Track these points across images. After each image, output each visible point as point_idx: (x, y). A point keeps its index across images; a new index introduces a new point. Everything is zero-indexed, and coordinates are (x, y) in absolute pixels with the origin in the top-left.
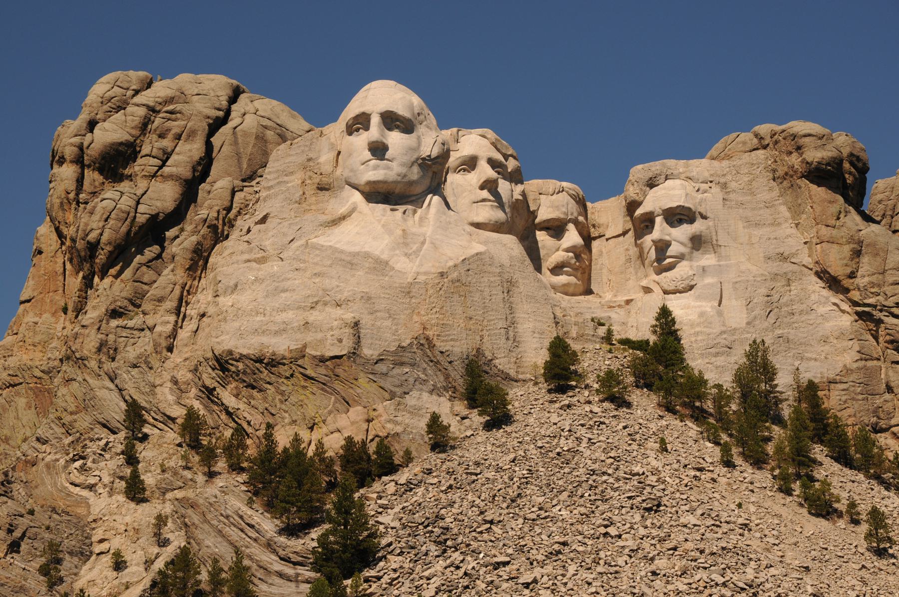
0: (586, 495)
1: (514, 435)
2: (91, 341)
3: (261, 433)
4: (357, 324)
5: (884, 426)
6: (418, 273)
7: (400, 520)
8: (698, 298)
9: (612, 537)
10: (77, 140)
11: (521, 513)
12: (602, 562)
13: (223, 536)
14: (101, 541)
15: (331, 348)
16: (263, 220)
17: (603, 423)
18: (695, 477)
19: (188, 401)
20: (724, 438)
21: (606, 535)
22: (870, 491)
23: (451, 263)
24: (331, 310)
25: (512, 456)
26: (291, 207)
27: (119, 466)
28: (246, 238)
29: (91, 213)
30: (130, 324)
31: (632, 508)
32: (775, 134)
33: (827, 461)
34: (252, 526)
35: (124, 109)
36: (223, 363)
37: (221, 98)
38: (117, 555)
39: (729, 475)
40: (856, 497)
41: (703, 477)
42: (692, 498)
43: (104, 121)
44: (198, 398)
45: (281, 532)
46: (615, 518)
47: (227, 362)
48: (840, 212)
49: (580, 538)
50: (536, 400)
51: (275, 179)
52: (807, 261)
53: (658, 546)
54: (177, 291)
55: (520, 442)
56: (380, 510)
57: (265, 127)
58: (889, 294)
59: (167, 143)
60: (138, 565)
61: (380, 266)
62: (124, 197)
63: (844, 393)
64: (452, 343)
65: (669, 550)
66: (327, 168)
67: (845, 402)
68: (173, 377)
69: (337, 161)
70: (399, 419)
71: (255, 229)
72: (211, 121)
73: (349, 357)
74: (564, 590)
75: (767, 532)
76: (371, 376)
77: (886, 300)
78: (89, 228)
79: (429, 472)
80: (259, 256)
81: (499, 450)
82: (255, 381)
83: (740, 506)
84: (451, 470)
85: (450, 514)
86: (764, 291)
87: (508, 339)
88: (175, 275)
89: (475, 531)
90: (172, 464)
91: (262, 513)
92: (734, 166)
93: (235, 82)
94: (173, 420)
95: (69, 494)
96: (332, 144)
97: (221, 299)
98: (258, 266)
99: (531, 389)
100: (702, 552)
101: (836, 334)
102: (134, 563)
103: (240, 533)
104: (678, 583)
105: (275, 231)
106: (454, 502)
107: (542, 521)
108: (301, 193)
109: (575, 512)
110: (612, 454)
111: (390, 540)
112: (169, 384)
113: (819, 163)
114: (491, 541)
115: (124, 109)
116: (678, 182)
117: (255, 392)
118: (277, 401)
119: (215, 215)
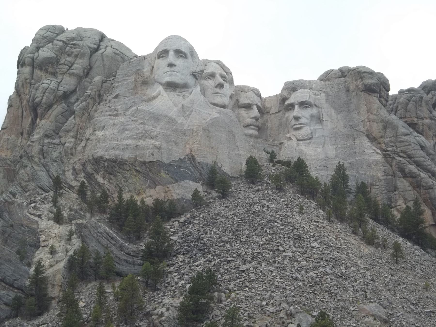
0: (268, 231)
2: (36, 149)
3: (115, 195)
5: (393, 206)
6: (189, 125)
7: (182, 238)
9: (281, 251)
10: (31, 55)
12: (277, 262)
13: (99, 242)
14: (44, 241)
16: (117, 97)
17: (272, 198)
19: (80, 179)
21: (278, 250)
23: (204, 122)
24: (148, 140)
25: (233, 212)
27: (51, 207)
28: (108, 105)
29: (37, 89)
30: (54, 142)
31: (289, 238)
33: (370, 220)
35: (52, 42)
36: (97, 161)
37: (96, 39)
38: (52, 247)
39: (330, 225)
40: (385, 237)
42: (316, 235)
43: (43, 47)
44: (84, 177)
49: (266, 251)
50: (242, 187)
52: (362, 129)
53: (302, 256)
54: (76, 128)
57: (116, 54)
60: (61, 253)
61: (171, 121)
62: (52, 83)
65: (307, 258)
66: (147, 74)
67: (377, 194)
68: (73, 167)
69: (152, 71)
70: (179, 192)
74: (260, 274)
75: (349, 251)
76: (166, 172)
77: (397, 148)
78: (36, 96)
79: (194, 217)
80: (115, 113)
81: (226, 209)
83: (336, 239)
86: (343, 142)
88: (75, 120)
90: (75, 207)
92: (331, 84)
94: (73, 187)
95: (29, 219)
96: (150, 63)
97: (97, 132)
100: (321, 259)
102: (59, 251)
103: (107, 241)
104: (311, 273)
106: (207, 232)
109: (263, 239)
111: (178, 248)
112: (71, 171)
113: (370, 85)
114: (225, 250)
115: (52, 42)
116: (306, 90)
117: (112, 177)
119: (94, 93)
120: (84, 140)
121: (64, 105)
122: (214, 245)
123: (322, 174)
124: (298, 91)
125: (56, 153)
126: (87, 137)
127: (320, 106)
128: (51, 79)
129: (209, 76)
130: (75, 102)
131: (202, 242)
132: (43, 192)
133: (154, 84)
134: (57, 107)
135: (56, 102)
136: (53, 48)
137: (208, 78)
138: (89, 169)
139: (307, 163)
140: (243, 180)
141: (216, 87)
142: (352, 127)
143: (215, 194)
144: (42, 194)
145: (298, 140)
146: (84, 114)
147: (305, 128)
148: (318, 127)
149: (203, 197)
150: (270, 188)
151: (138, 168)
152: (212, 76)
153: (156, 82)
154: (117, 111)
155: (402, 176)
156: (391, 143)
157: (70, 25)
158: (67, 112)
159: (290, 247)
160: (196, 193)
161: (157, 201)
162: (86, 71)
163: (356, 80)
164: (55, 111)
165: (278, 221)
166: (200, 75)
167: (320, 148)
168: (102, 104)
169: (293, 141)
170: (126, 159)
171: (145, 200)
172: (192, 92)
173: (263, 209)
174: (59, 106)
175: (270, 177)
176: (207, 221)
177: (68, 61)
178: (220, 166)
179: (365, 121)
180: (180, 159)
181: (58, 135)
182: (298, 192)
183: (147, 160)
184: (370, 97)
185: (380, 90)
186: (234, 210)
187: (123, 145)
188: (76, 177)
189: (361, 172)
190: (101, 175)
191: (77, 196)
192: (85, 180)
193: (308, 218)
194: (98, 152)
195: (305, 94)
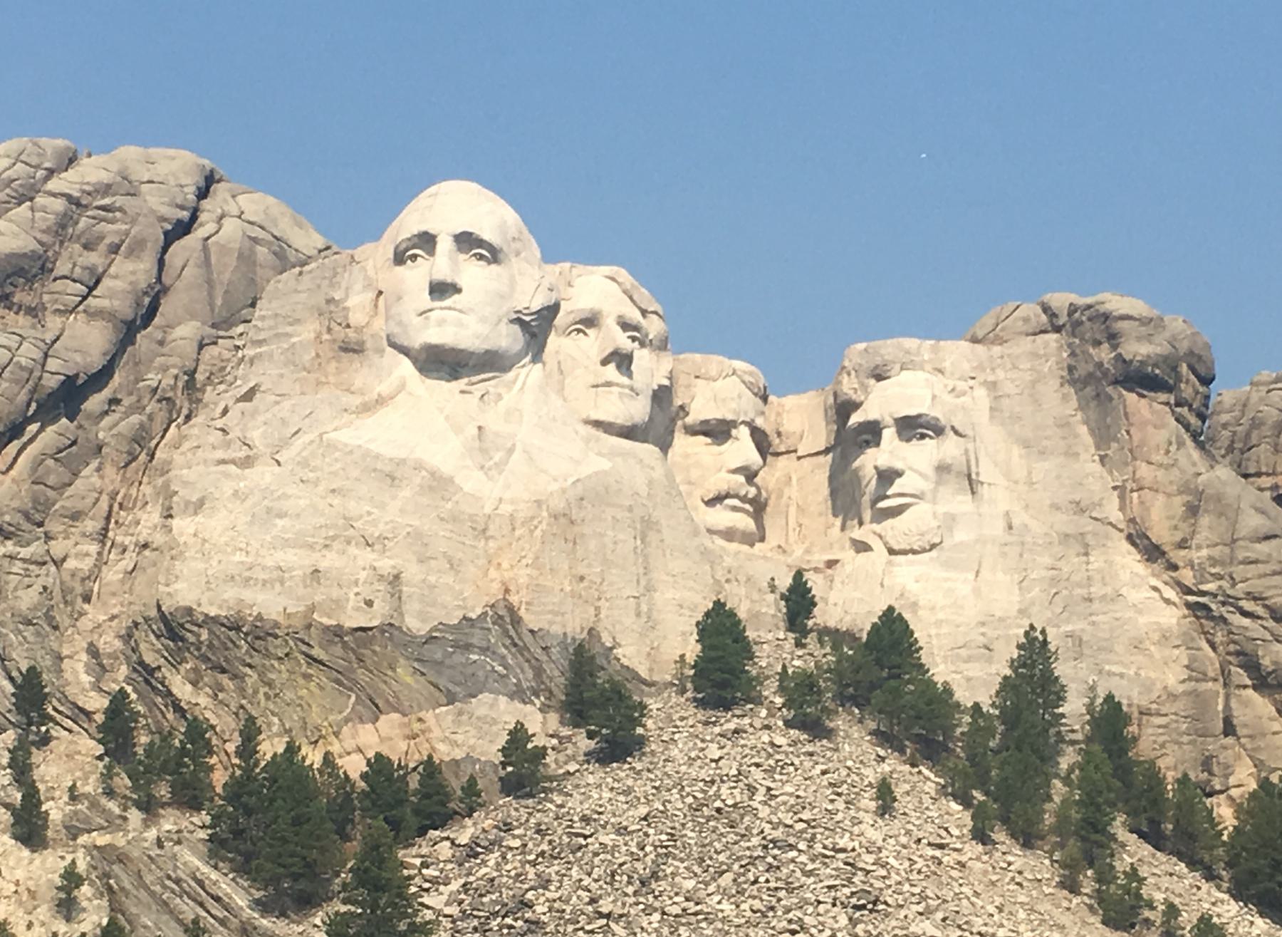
0: (762, 879)
1: (645, 774)
3: (231, 747)
4: (397, 577)
5: (1218, 787)
7: (461, 903)
8: (947, 565)
11: (657, 904)
13: (171, 912)
15: (355, 614)
16: (249, 396)
18: (933, 857)
20: (978, 795)
22: (1195, 890)
23: (555, 487)
24: (356, 552)
25: (643, 810)
26: (296, 376)
28: (219, 424)
30: (25, 552)
31: (834, 905)
32: (1076, 311)
34: (217, 899)
35: (31, 199)
39: (985, 858)
40: (1177, 901)
41: (945, 860)
44: (129, 680)
45: (263, 907)
46: (807, 919)
47: (182, 626)
48: (1170, 443)
51: (271, 328)
56: (427, 885)
57: (255, 240)
58: (1238, 579)
59: (95, 258)
61: (439, 484)
62: (25, 344)
63: (1161, 731)
64: (550, 616)
67: (1163, 746)
68: (91, 644)
69: (376, 306)
71: (236, 410)
72: (169, 227)
73: (383, 632)
76: (416, 665)
79: (507, 827)
81: (622, 798)
82: (227, 660)
84: (543, 827)
85: (542, 900)
86: (1047, 560)
87: (638, 615)
88: (102, 477)
89: (582, 929)
90: (89, 789)
91: (233, 880)
92: (1009, 355)
93: (207, 162)
94: (89, 715)
97: (176, 523)
98: (239, 471)
99: (674, 700)
101: (1156, 636)
105: (269, 415)
106: (549, 881)
107: (693, 919)
108: (313, 354)
110: (806, 815)
112: (84, 657)
115: (31, 199)
116: (920, 375)
117: (225, 680)
118: (261, 696)
119: (172, 382)
120: (132, 547)
123: (967, 672)
127: (970, 433)
129: (576, 323)
131: (527, 915)
136: (33, 219)
140: (689, 694)
141: (605, 362)
142: (1079, 508)
145: (892, 552)
148: (960, 503)
151: (317, 652)
152: (590, 321)
155: (1249, 682)
156: (1213, 566)
160: (518, 736)
161: (379, 766)
162: (147, 300)
168: (198, 420)
170: (274, 617)
171: (339, 762)
173: (751, 799)
176: (550, 842)
177: (84, 268)
178: (609, 645)
180: (465, 618)
183: (350, 623)
184: (1143, 401)
185: (1179, 378)
187: (264, 568)
188: (98, 681)
189: (1107, 667)
190: (187, 671)
191: (100, 750)
192: (129, 689)
193: (908, 833)
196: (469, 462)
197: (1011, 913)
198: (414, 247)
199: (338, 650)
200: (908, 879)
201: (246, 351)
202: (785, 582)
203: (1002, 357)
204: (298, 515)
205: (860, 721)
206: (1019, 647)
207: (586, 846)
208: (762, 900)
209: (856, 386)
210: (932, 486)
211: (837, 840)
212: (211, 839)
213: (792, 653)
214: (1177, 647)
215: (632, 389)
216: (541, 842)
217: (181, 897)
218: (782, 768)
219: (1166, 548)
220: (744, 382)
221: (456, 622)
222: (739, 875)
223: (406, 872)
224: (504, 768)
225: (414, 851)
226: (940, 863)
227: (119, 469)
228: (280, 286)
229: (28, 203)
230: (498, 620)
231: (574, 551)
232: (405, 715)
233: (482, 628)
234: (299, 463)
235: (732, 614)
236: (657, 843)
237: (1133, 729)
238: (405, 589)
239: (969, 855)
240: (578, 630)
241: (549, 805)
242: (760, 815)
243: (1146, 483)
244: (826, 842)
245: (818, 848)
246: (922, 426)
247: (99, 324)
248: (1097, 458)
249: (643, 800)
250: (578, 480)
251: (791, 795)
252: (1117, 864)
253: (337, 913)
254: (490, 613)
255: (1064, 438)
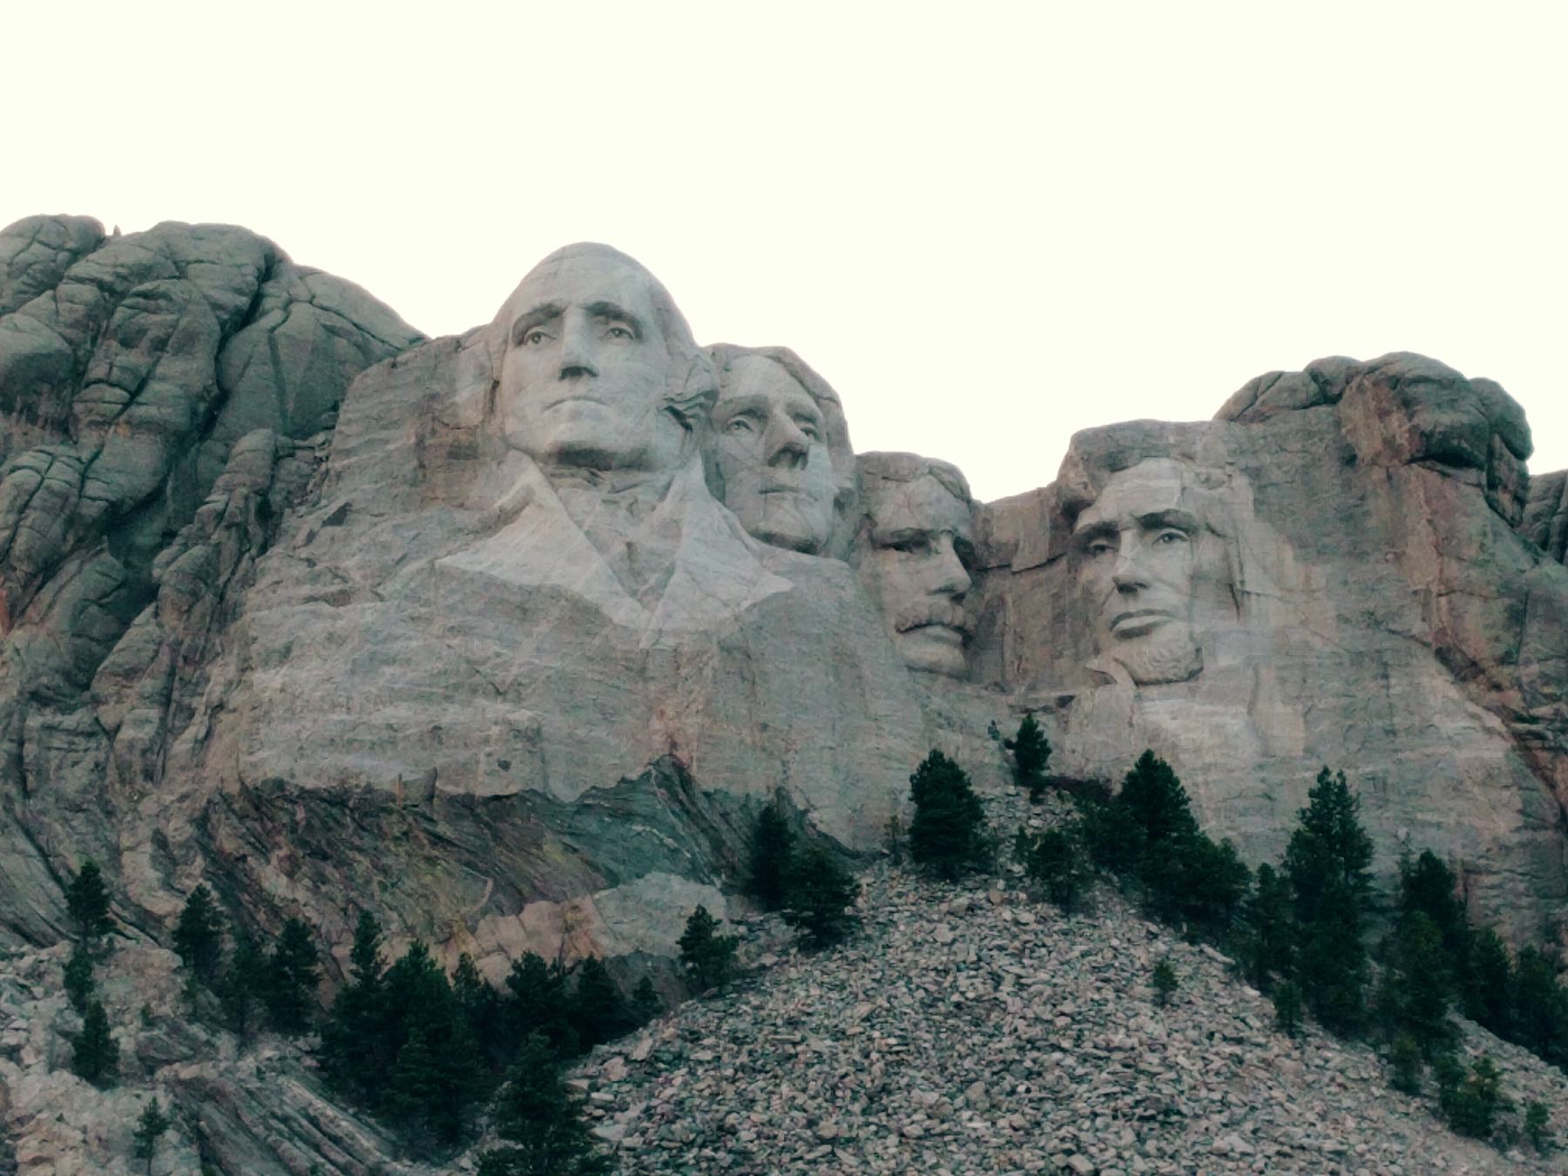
0: (1021, 1089)
1: (861, 965)
3: (343, 951)
6: (660, 631)
7: (643, 1133)
11: (893, 1124)
13: (279, 1159)
15: (487, 780)
16: (339, 518)
19: (187, 882)
22: (1557, 1088)
23: (726, 614)
25: (864, 1009)
26: (395, 491)
27: (61, 1011)
28: (304, 553)
31: (1115, 1118)
33: (1470, 1027)
35: (53, 287)
36: (262, 803)
37: (244, 270)
39: (1296, 1054)
40: (1540, 1100)
42: (1232, 1098)
43: (14, 311)
46: (1083, 1136)
50: (900, 895)
51: (359, 435)
52: (1418, 627)
54: (165, 657)
55: (878, 981)
56: (600, 1112)
57: (332, 331)
59: (135, 358)
61: (583, 616)
62: (57, 464)
63: (1494, 892)
66: (471, 416)
67: (1496, 911)
68: (157, 832)
69: (492, 401)
72: (226, 317)
76: (567, 840)
79: (694, 1037)
81: (835, 995)
82: (329, 844)
84: (741, 1035)
86: (1336, 685)
88: (160, 625)
89: (801, 1158)
90: (166, 1010)
94: (159, 920)
97: (258, 677)
99: (886, 873)
101: (1480, 775)
103: (313, 1154)
105: (365, 540)
106: (753, 1101)
108: (415, 463)
110: (1068, 1007)
112: (148, 848)
113: (1445, 436)
115: (53, 287)
116: (1165, 464)
117: (328, 869)
118: (375, 887)
119: (241, 504)
120: (202, 709)
121: (107, 557)
122: (786, 1157)
124: (1132, 470)
125: (78, 771)
126: (215, 700)
127: (1230, 532)
128: (49, 449)
130: (160, 547)
131: (730, 1145)
132: (27, 947)
133: (505, 454)
134: (80, 571)
135: (73, 550)
136: (57, 312)
137: (738, 423)
138: (228, 840)
139: (1186, 778)
141: (773, 462)
142: (1373, 621)
143: (781, 931)
144: (22, 956)
145: (1139, 683)
146: (195, 596)
147: (1169, 627)
148: (1225, 623)
149: (734, 942)
150: (1023, 896)
151: (443, 829)
152: (756, 412)
153: (510, 447)
154: (344, 580)
156: (1546, 684)
157: (127, 214)
158: (123, 592)
159: (1119, 1156)
160: (700, 924)
162: (202, 407)
163: (1383, 414)
164: (70, 588)
165: (1066, 1044)
166: (702, 414)
167: (1235, 716)
168: (276, 550)
169: (1117, 689)
170: (387, 787)
171: (479, 965)
172: (668, 487)
173: (996, 989)
174: (87, 567)
175: (1019, 846)
176: (750, 1053)
177: (124, 369)
178: (801, 807)
179: (1428, 591)
180: (623, 780)
181: (87, 695)
182: (1147, 912)
184: (1449, 482)
185: (1491, 453)
186: (868, 998)
187: (371, 727)
188: (169, 875)
190: (280, 860)
191: (178, 961)
192: (208, 885)
194: (263, 760)
195: (1163, 483)
196: (619, 588)
197: (1336, 1121)
198: (539, 324)
199: (468, 825)
200: (1206, 1084)
201: (330, 465)
202: (1011, 728)
203: (1264, 437)
204: (408, 661)
205: (1121, 891)
206: (1312, 794)
207: (796, 1055)
208: (1023, 1114)
209: (1085, 479)
210: (1186, 599)
211: (1111, 1036)
212: (323, 1067)
213: (1028, 810)
214: (1507, 787)
215: (809, 494)
216: (739, 1052)
217: (290, 1140)
218: (1033, 951)
219: (1485, 664)
220: (942, 483)
221: (613, 784)
222: (993, 1084)
223: (571, 1098)
224: (683, 964)
225: (579, 1071)
226: (1241, 1061)
227: (181, 613)
228: (369, 381)
229: (49, 293)
230: (665, 781)
231: (754, 694)
232: (557, 902)
233: (647, 793)
234: (407, 597)
235: (952, 765)
236: (885, 1049)
237: (1458, 891)
238: (545, 745)
239: (1276, 1050)
240: (764, 791)
241: (744, 1007)
242: (1011, 1009)
243: (1456, 585)
244: (1100, 1040)
245: (1088, 1047)
246: (1170, 525)
247: (145, 438)
248: (1390, 556)
249: (861, 996)
250: (754, 605)
251: (1047, 983)
252: (1459, 1057)
253: (491, 1153)
254: (654, 772)
255: (1348, 534)
